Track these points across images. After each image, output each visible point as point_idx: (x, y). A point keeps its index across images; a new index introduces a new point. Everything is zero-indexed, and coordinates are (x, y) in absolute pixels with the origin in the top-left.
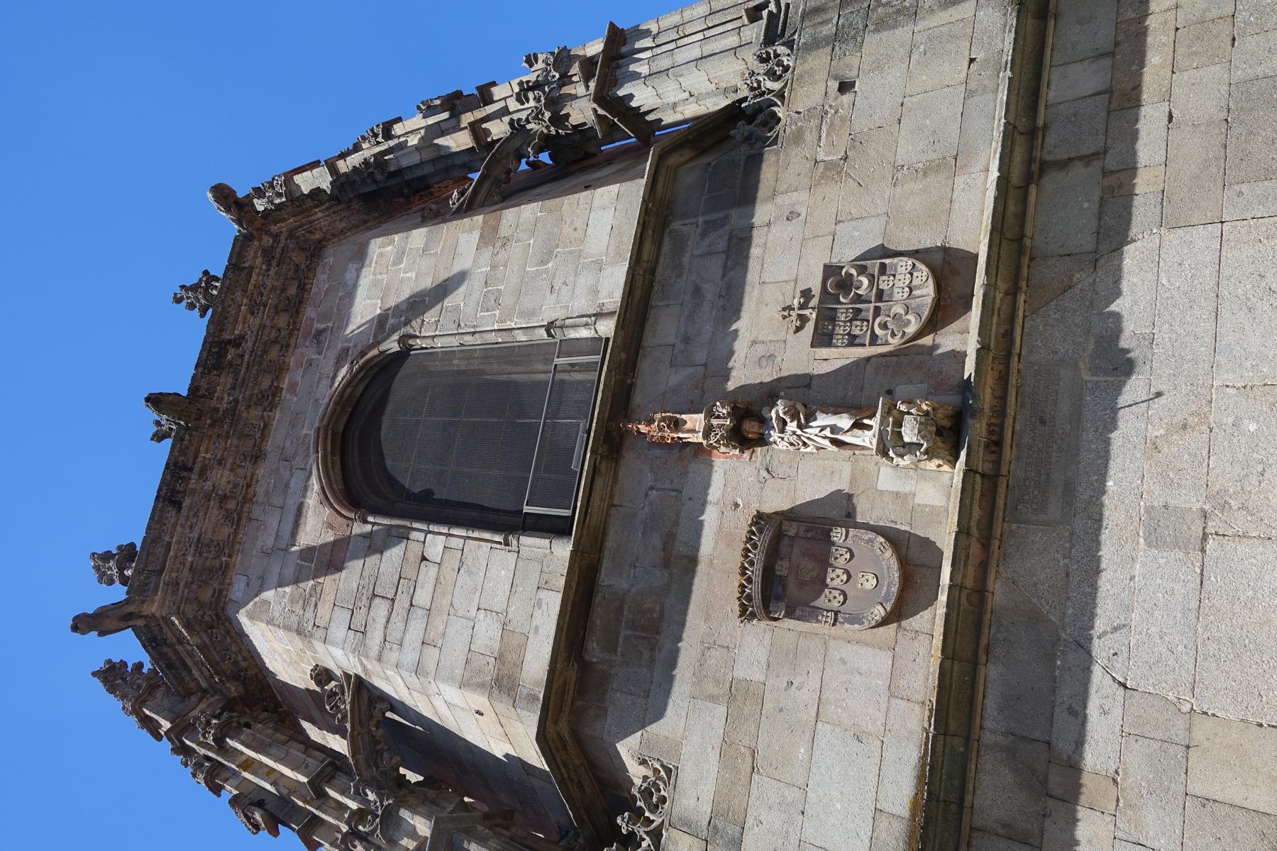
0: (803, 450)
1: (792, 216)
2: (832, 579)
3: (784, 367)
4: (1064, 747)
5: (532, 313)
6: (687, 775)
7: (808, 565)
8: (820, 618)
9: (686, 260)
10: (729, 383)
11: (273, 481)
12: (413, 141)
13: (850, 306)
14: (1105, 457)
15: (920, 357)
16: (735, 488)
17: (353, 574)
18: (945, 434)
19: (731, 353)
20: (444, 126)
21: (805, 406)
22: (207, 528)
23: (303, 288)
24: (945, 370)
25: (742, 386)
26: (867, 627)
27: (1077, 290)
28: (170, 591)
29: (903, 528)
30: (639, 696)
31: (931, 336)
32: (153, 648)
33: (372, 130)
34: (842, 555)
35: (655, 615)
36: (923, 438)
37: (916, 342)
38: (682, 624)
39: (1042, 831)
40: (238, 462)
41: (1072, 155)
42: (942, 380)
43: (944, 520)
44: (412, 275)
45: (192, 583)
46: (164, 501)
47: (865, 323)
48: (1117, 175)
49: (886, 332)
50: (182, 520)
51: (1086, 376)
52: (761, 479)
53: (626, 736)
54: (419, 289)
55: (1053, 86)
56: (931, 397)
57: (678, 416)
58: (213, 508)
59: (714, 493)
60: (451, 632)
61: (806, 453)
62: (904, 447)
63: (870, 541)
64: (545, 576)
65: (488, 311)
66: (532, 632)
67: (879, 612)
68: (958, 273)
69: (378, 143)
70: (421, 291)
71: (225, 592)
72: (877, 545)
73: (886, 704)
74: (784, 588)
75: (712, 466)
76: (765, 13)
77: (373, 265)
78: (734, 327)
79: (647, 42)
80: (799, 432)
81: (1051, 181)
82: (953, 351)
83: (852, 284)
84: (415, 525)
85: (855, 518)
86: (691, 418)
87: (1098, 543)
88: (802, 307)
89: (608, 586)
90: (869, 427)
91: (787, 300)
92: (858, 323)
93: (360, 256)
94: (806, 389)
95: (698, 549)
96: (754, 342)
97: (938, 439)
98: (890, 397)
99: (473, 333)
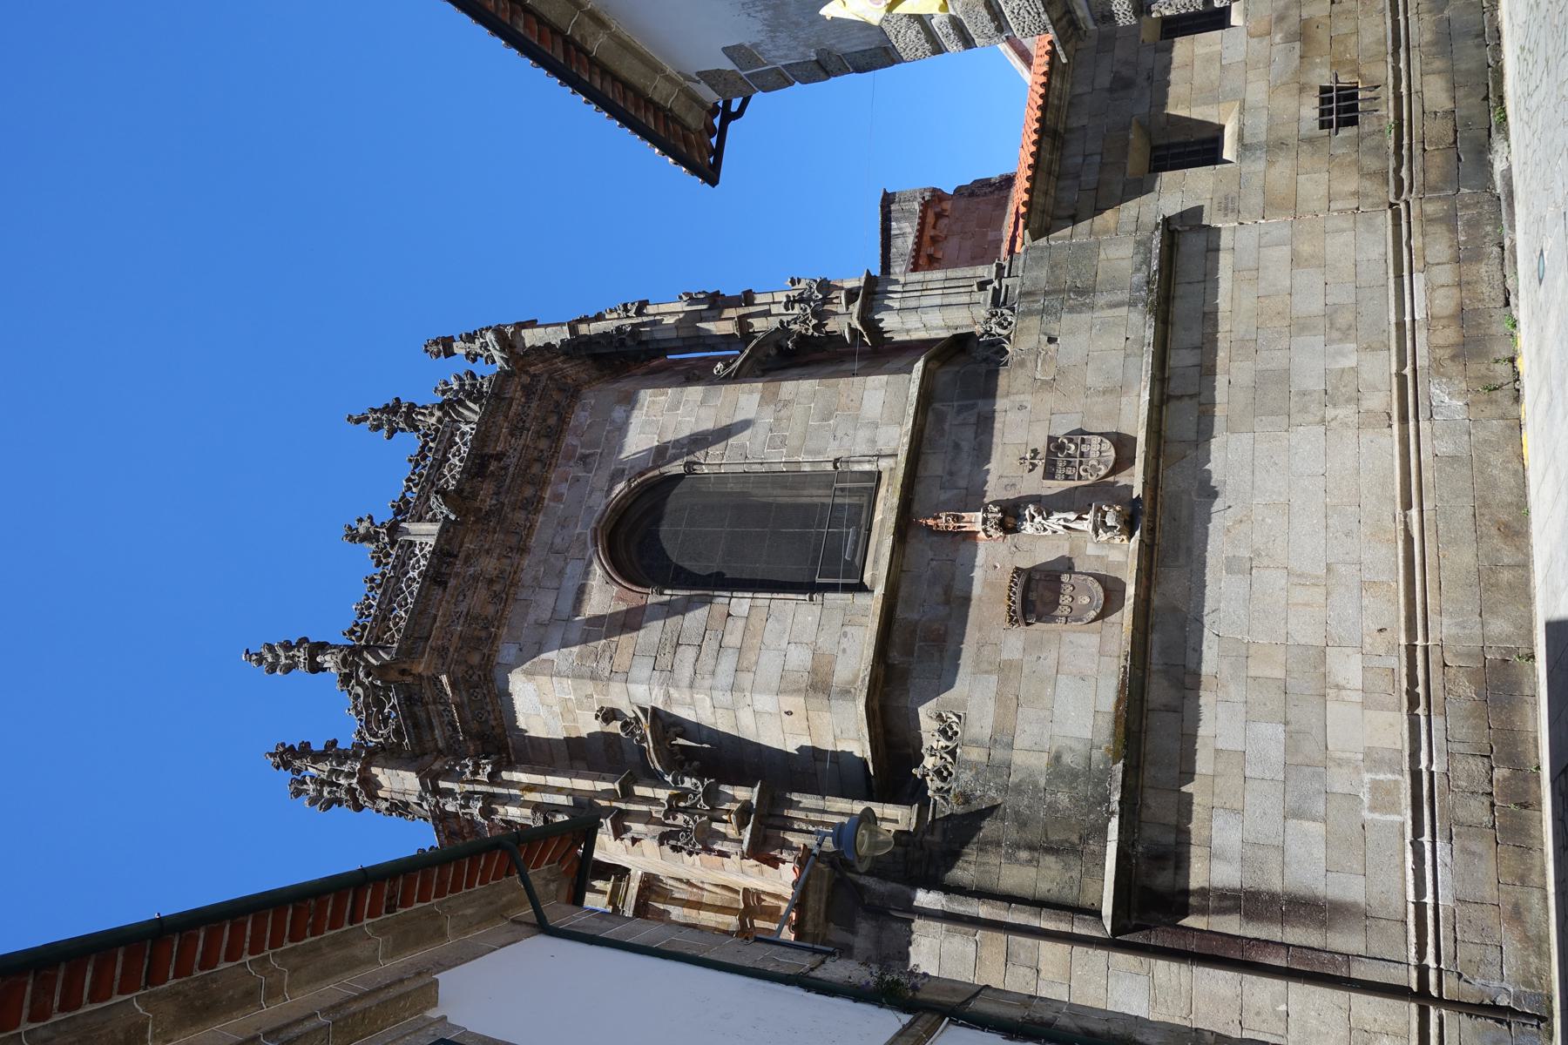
0: (1042, 533)
1: (1021, 407)
4: (1191, 665)
6: (972, 714)
7: (1048, 595)
9: (947, 426)
11: (542, 569)
12: (669, 320)
14: (1206, 536)
17: (653, 632)
19: (986, 482)
20: (704, 314)
23: (563, 420)
32: (407, 706)
33: (625, 305)
38: (963, 635)
44: (693, 420)
45: (461, 648)
50: (447, 597)
51: (1195, 499)
53: (925, 702)
54: (701, 429)
59: (980, 560)
60: (764, 660)
64: (848, 618)
66: (840, 653)
67: (1093, 614)
69: (628, 317)
70: (703, 431)
74: (1034, 606)
76: (990, 287)
77: (645, 408)
78: (986, 467)
79: (898, 288)
80: (1043, 522)
81: (1173, 405)
84: (716, 593)
87: (1204, 575)
88: (1032, 458)
93: (630, 401)
95: (971, 593)
96: (1001, 477)
99: (762, 463)
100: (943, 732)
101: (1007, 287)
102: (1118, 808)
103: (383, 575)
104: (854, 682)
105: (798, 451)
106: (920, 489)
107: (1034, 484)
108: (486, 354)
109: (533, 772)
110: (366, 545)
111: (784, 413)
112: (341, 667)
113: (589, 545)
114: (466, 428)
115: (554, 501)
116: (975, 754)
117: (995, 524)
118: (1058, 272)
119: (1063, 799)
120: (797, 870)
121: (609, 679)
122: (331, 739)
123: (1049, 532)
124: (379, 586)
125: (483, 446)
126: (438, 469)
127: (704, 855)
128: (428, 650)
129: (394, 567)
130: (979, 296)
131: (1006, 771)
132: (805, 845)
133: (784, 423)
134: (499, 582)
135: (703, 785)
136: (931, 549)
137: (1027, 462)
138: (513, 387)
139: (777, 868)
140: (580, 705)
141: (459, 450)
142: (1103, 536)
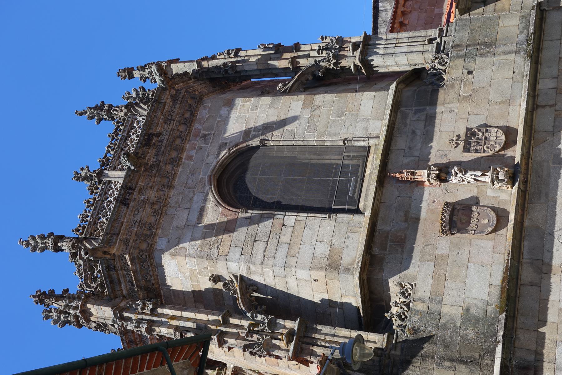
0: (462, 183)
1: (451, 111)
2: (473, 221)
4: (546, 260)
5: (335, 135)
6: (419, 284)
7: (464, 218)
8: (469, 232)
9: (408, 121)
11: (181, 197)
12: (253, 59)
14: (557, 186)
17: (241, 233)
19: (430, 153)
20: (272, 56)
22: (144, 216)
23: (193, 115)
27: (548, 141)
28: (122, 243)
30: (397, 263)
31: (503, 151)
32: (107, 271)
33: (228, 51)
35: (402, 237)
37: (499, 153)
38: (415, 239)
39: (541, 282)
40: (161, 188)
41: (546, 104)
44: (265, 116)
45: (136, 240)
46: (120, 202)
48: (559, 111)
50: (129, 212)
51: (551, 165)
53: (393, 277)
54: (269, 121)
55: (540, 84)
58: (147, 208)
59: (425, 197)
60: (302, 250)
65: (310, 132)
67: (490, 229)
68: (512, 134)
69: (230, 57)
70: (270, 122)
71: (153, 246)
72: (488, 211)
73: (492, 255)
74: (456, 224)
76: (435, 42)
77: (239, 109)
78: (430, 145)
79: (382, 42)
80: (462, 176)
81: (540, 111)
82: (511, 156)
84: (276, 213)
86: (419, 172)
87: (556, 208)
88: (457, 140)
89: (381, 229)
92: (479, 146)
93: (230, 105)
95: (420, 215)
96: (438, 150)
99: (303, 141)
100: (403, 294)
101: (445, 42)
102: (502, 340)
103: (95, 199)
104: (353, 264)
105: (323, 134)
106: (392, 156)
107: (458, 155)
108: (151, 78)
109: (174, 309)
110: (85, 182)
111: (316, 112)
112: (71, 249)
113: (207, 184)
114: (140, 119)
115: (188, 160)
116: (420, 307)
117: (435, 177)
118: (475, 33)
119: (470, 333)
120: (319, 368)
121: (217, 259)
122: (66, 288)
123: (466, 182)
124: (92, 205)
125: (150, 129)
126: (125, 141)
127: (267, 358)
128: (118, 240)
129: (100, 195)
130: (429, 47)
131: (438, 317)
132: (324, 354)
133: (316, 118)
134: (157, 204)
135: (268, 319)
136: (398, 190)
137: (454, 142)
138: (166, 96)
139: (308, 366)
140: (201, 273)
141: (136, 131)
142: (497, 185)
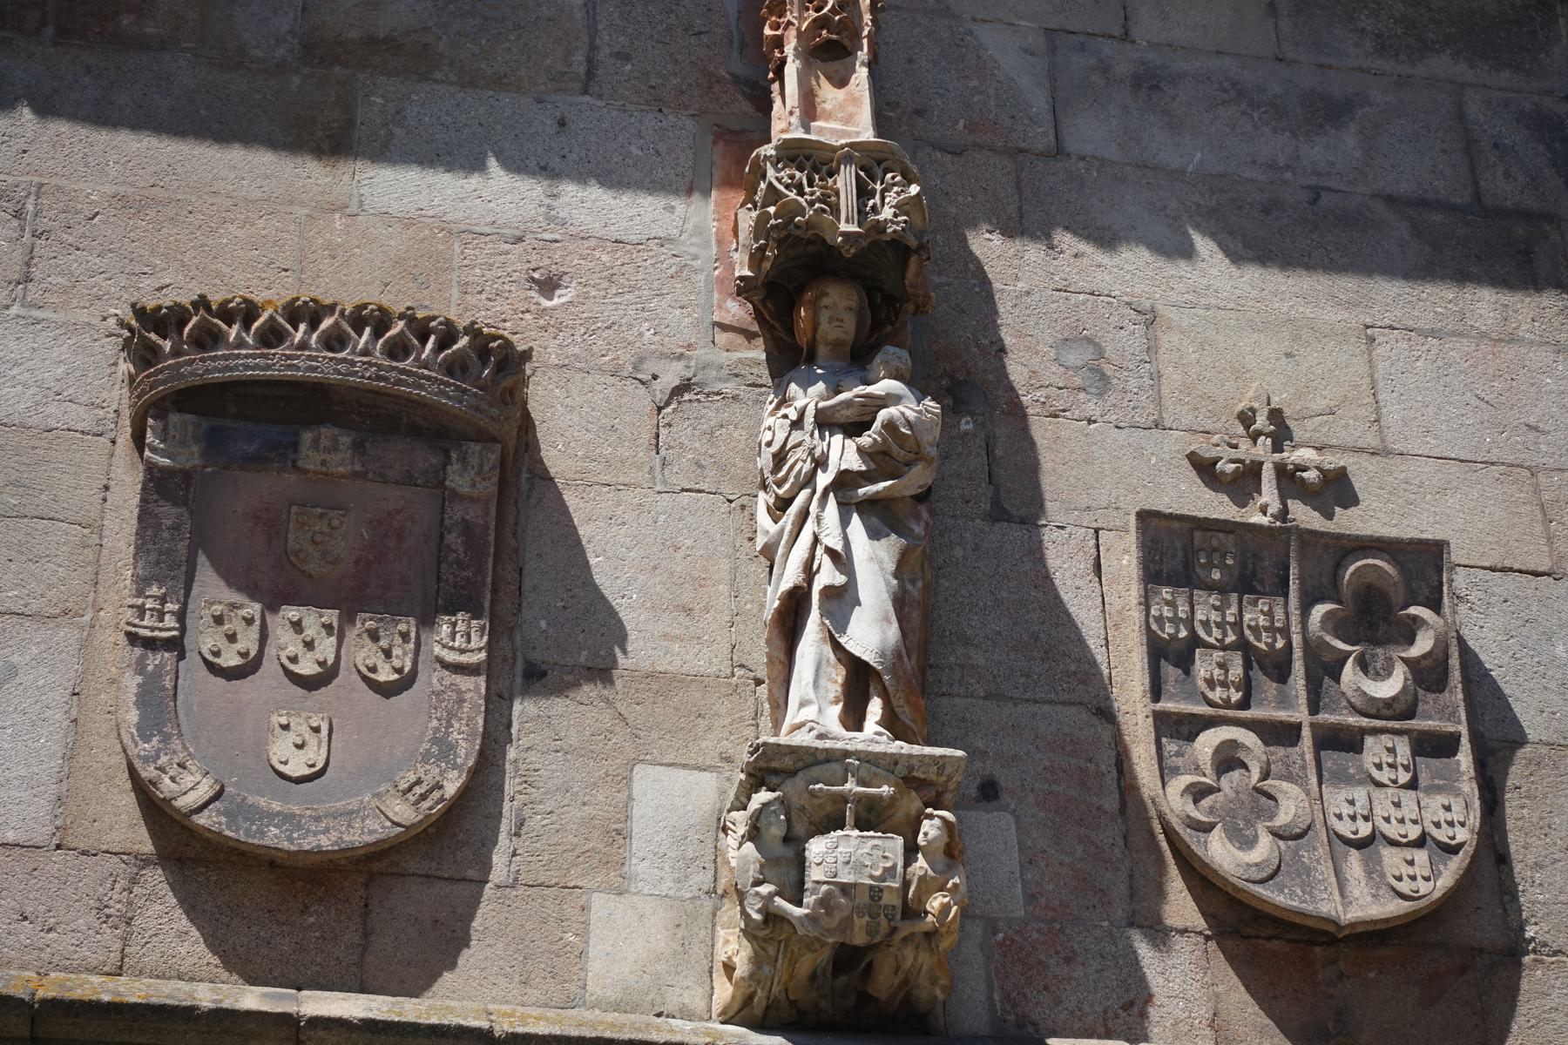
0: (763, 500)
2: (297, 626)
3: (1068, 428)
8: (155, 590)
9: (1441, 65)
10: (997, 239)
13: (1296, 639)
15: (1123, 888)
16: (610, 279)
18: (843, 979)
19: (1107, 240)
21: (921, 498)
24: (1079, 972)
25: (985, 282)
26: (133, 751)
29: (499, 859)
31: (1199, 922)
34: (388, 654)
35: (126, 20)
36: (825, 902)
38: (102, 116)
42: (1041, 963)
43: (534, 994)
47: (1236, 696)
49: (1208, 771)
52: (650, 367)
56: (977, 929)
57: (863, 55)
61: (753, 517)
62: (787, 840)
63: (445, 750)
72: (431, 773)
74: (255, 462)
75: (689, 192)
78: (1204, 245)
80: (824, 480)
82: (1149, 998)
83: (1377, 643)
85: (527, 692)
86: (855, 101)
88: (1288, 478)
90: (854, 718)
91: (1309, 423)
92: (1236, 672)
94: (986, 506)
96: (1150, 318)
97: (825, 955)
98: (973, 791)
